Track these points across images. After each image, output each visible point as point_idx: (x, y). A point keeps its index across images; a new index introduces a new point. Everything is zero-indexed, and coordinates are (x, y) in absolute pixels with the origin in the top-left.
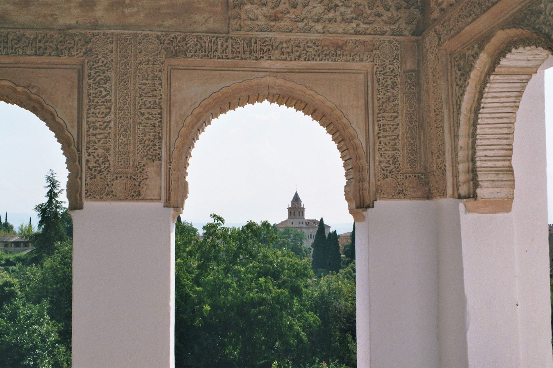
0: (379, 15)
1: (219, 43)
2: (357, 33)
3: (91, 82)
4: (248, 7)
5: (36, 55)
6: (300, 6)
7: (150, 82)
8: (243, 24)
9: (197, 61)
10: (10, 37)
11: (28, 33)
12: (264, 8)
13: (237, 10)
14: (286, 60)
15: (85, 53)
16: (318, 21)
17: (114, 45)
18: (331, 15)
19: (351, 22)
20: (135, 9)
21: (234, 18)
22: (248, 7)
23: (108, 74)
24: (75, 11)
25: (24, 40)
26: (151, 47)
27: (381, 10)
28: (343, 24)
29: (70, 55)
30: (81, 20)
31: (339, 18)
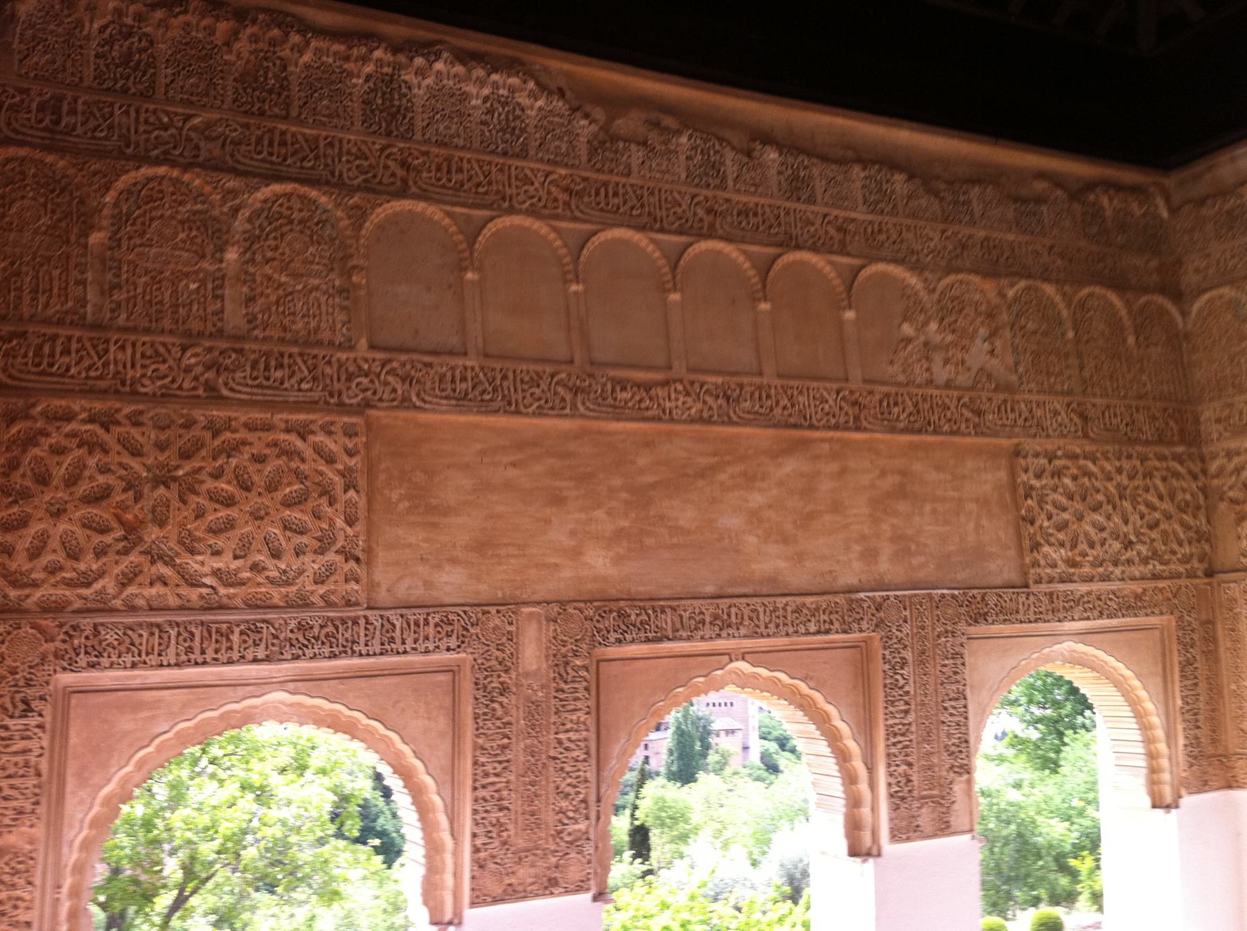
0: (1174, 553)
1: (1021, 601)
2: (1155, 577)
3: (887, 666)
4: (1046, 549)
5: (819, 632)
6: (1098, 546)
7: (951, 661)
8: (1043, 575)
9: (996, 628)
10: (789, 609)
11: (808, 600)
12: (1062, 551)
13: (1035, 554)
14: (1088, 619)
15: (877, 626)
16: (1116, 564)
17: (907, 613)
18: (1128, 554)
19: (1147, 563)
20: (922, 559)
21: (1033, 566)
22: (1046, 549)
23: (904, 654)
24: (857, 565)
25: (805, 611)
26: (950, 611)
27: (1175, 546)
28: (1142, 568)
29: (861, 631)
30: (864, 577)
31: (1137, 560)
